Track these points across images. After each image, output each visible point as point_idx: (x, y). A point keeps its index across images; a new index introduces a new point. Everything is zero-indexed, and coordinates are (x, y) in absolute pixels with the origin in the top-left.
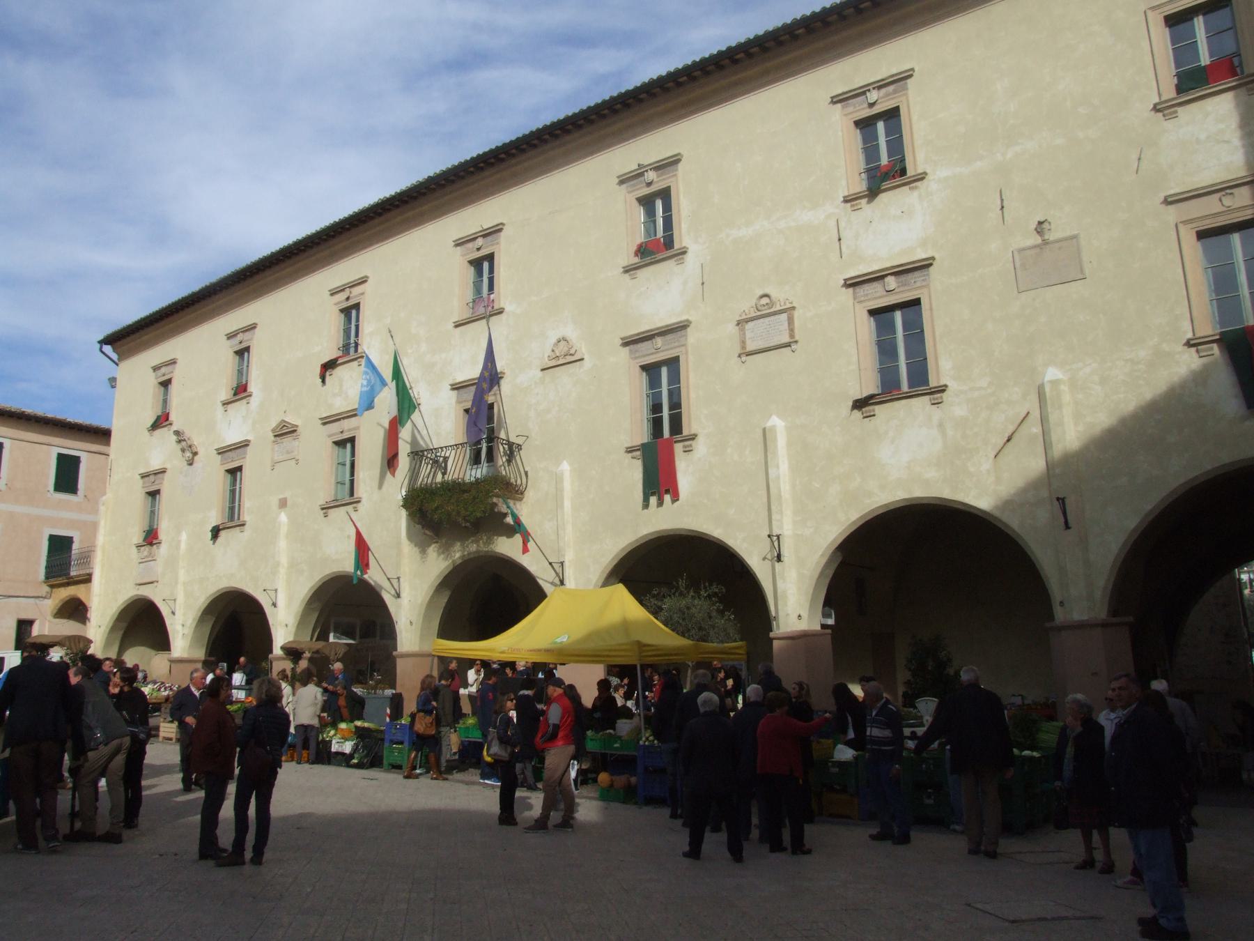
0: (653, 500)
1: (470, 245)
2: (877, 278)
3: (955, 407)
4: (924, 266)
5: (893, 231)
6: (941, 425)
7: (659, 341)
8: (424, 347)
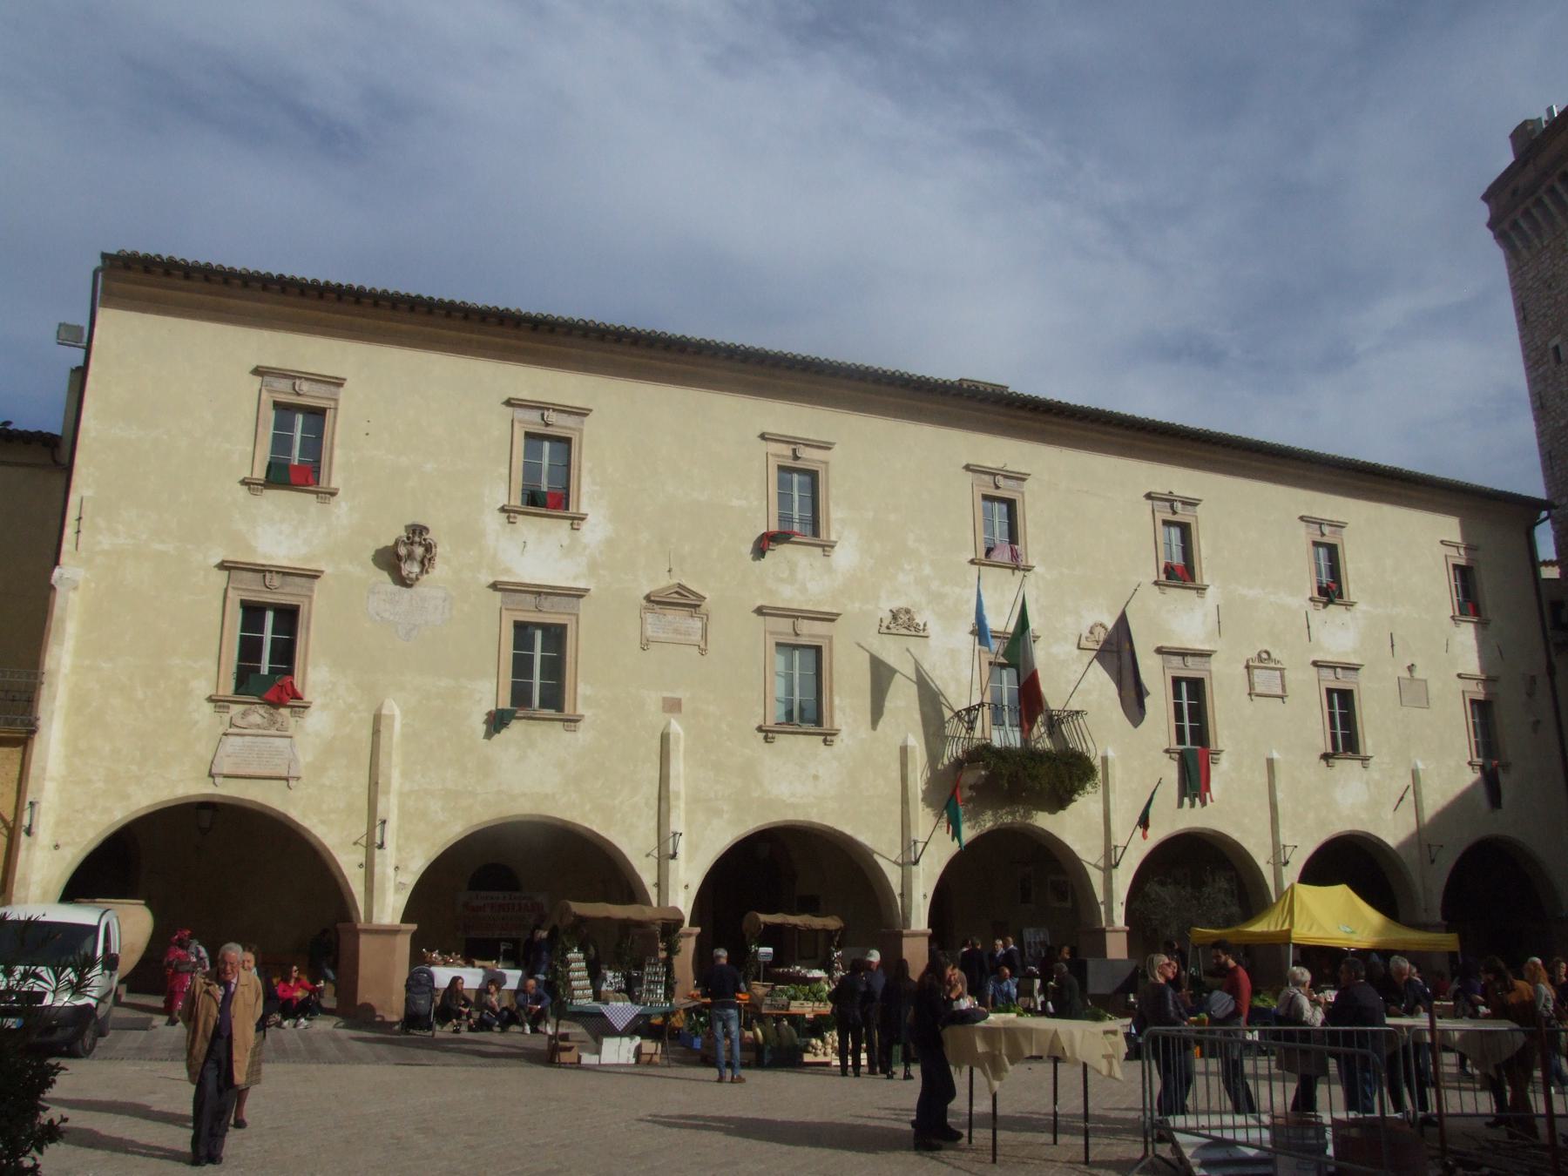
0: (1186, 800)
1: (987, 478)
2: (1333, 667)
3: (1374, 772)
4: (1354, 668)
5: (1338, 635)
6: (1367, 783)
7: (1189, 660)
8: (927, 570)
